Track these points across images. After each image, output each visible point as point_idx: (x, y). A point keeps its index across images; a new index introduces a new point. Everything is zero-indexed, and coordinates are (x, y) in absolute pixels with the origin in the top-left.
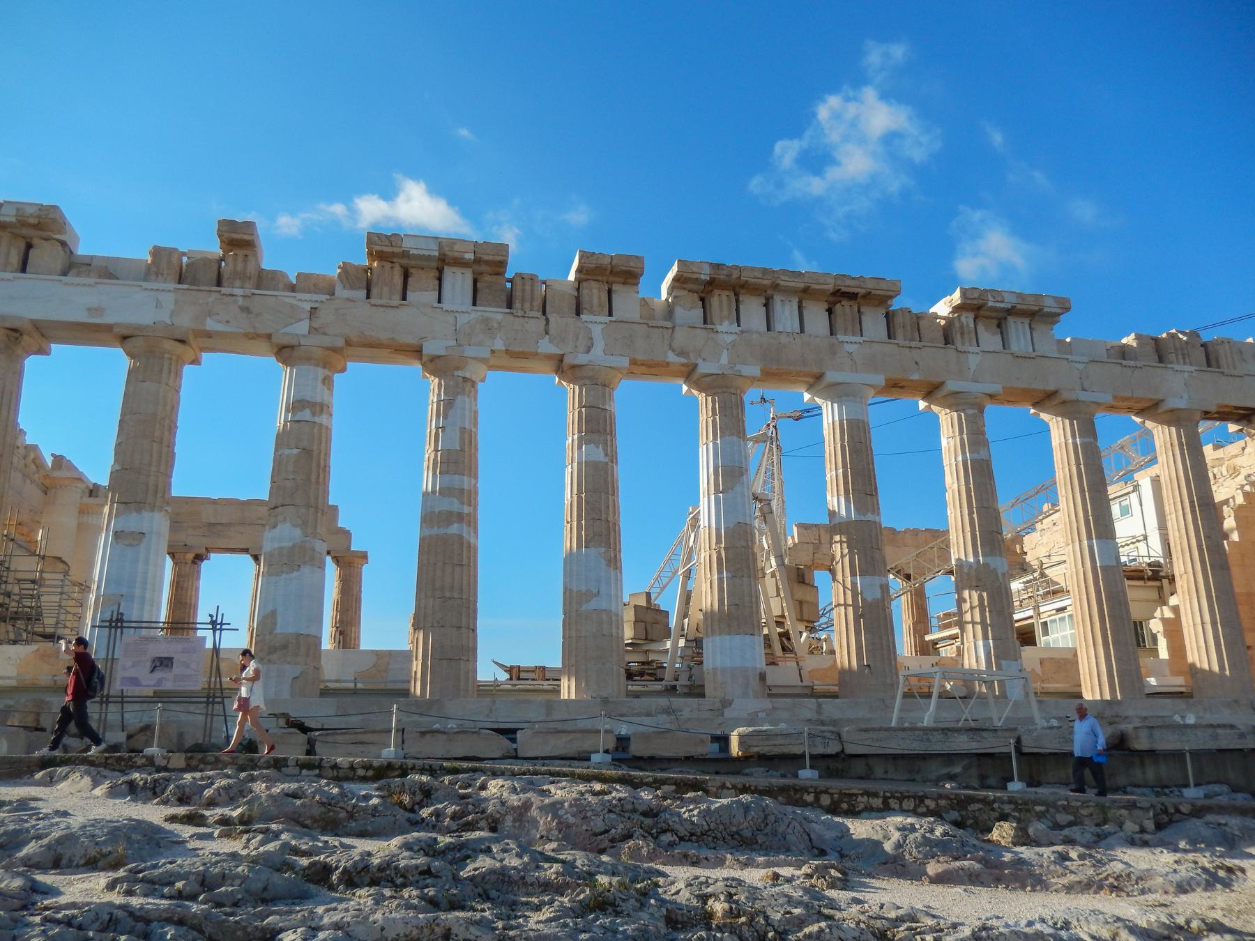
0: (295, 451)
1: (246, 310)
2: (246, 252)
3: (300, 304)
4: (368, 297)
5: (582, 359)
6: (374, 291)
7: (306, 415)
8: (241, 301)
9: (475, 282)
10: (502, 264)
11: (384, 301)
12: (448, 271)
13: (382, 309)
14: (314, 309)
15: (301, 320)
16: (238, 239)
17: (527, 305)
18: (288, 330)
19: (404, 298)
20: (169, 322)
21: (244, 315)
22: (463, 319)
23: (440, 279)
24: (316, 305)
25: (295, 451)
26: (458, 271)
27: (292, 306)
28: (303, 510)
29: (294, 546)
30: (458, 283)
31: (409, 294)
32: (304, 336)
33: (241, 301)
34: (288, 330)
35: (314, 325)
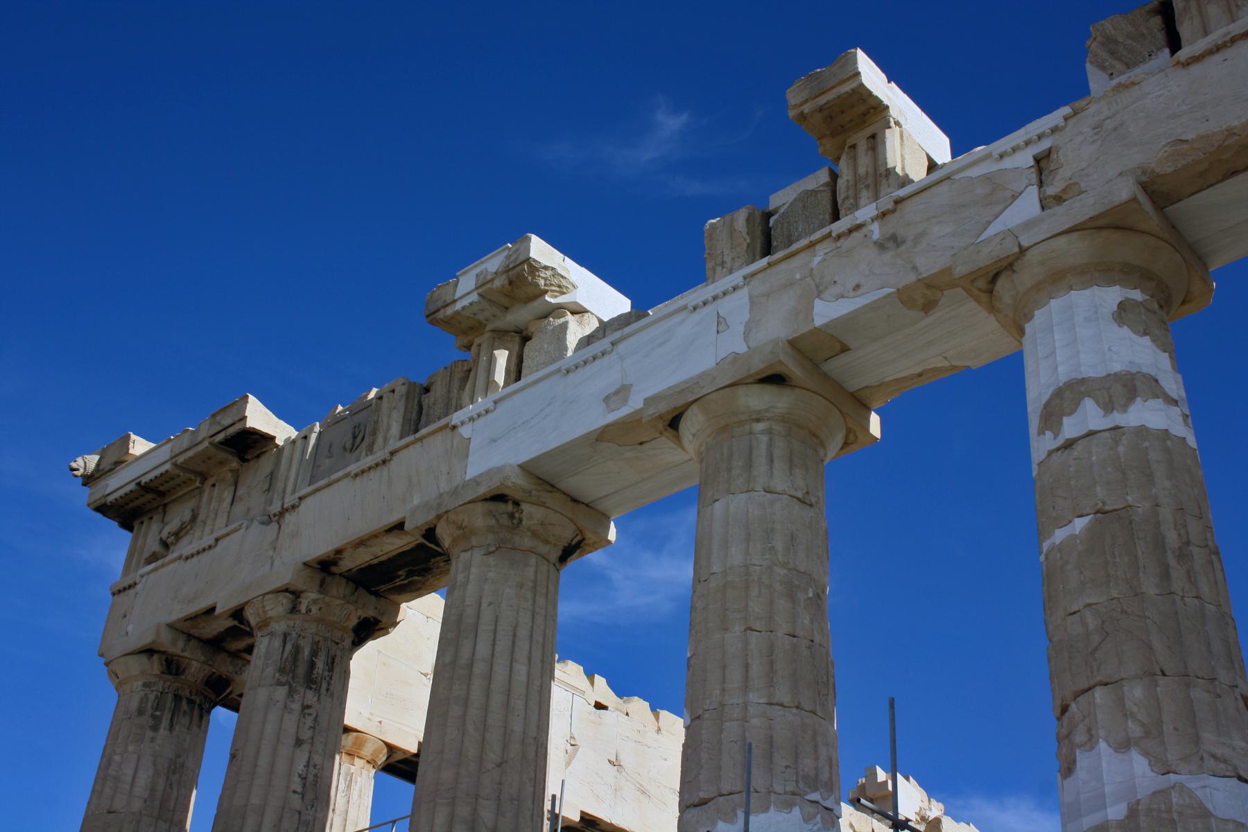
0: (1079, 524)
1: (893, 241)
2: (869, 131)
3: (1007, 163)
8: (876, 231)
11: (1216, 36)
13: (1217, 58)
14: (1041, 161)
15: (1015, 197)
21: (888, 256)
24: (1045, 145)
25: (1079, 524)
27: (987, 178)
28: (1136, 692)
29: (1133, 813)
32: (1029, 225)
33: (876, 231)
34: (991, 230)
35: (1051, 190)
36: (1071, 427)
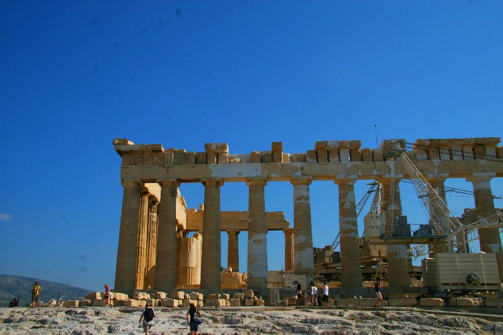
0: (302, 213)
4: (317, 161)
5: (387, 176)
6: (320, 159)
7: (303, 201)
9: (350, 152)
10: (359, 146)
12: (341, 150)
16: (277, 148)
17: (368, 159)
18: (295, 174)
19: (328, 161)
20: (260, 175)
22: (348, 166)
23: (339, 153)
26: (345, 150)
30: (345, 155)
31: (330, 159)
34: (295, 174)
36: (301, 201)
